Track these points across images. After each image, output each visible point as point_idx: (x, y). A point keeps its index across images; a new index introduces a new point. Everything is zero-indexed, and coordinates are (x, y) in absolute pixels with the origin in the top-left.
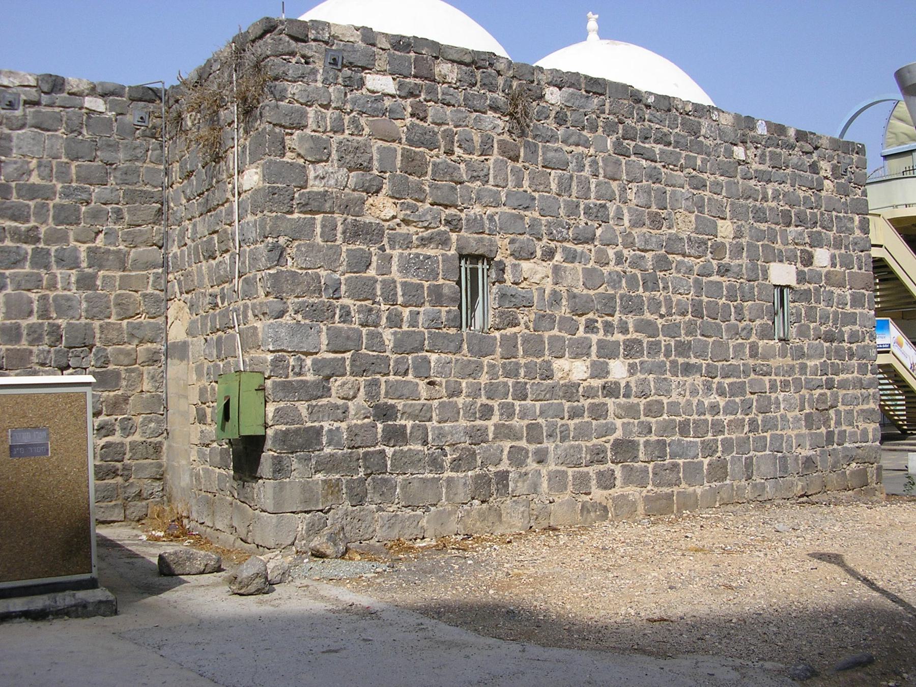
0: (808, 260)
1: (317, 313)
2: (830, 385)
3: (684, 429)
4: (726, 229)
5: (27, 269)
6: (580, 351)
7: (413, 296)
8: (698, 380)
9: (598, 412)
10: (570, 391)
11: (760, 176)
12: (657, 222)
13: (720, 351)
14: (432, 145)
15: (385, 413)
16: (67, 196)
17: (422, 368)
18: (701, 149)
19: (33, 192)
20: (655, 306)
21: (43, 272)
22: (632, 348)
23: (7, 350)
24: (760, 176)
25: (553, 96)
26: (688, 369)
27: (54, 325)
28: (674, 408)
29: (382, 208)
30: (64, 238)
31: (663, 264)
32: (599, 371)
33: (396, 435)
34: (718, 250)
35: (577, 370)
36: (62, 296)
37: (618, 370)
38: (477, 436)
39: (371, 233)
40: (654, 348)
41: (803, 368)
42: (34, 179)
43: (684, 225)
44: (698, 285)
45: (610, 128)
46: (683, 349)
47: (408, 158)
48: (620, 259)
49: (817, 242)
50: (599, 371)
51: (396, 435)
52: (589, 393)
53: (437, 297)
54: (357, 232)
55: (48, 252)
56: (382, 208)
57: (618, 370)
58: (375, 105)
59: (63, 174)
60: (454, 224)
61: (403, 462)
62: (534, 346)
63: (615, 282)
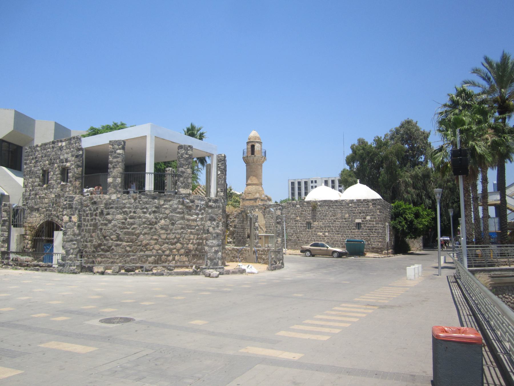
0: (365, 218)
1: (291, 229)
2: (369, 237)
3: (337, 241)
4: (347, 216)
6: (321, 232)
7: (301, 226)
8: (340, 235)
10: (320, 236)
11: (354, 208)
12: (334, 216)
13: (345, 232)
17: (302, 234)
18: (342, 206)
20: (333, 226)
22: (329, 232)
24: (354, 208)
25: (319, 203)
26: (338, 234)
28: (335, 239)
31: (335, 221)
32: (323, 234)
33: (299, 240)
35: (321, 234)
37: (327, 234)
38: (308, 240)
39: (297, 221)
40: (333, 231)
41: (362, 234)
43: (339, 216)
44: (341, 224)
46: (337, 231)
51: (299, 240)
53: (304, 227)
54: (295, 221)
56: (298, 218)
57: (327, 234)
58: (298, 209)
62: (315, 231)
63: (327, 224)
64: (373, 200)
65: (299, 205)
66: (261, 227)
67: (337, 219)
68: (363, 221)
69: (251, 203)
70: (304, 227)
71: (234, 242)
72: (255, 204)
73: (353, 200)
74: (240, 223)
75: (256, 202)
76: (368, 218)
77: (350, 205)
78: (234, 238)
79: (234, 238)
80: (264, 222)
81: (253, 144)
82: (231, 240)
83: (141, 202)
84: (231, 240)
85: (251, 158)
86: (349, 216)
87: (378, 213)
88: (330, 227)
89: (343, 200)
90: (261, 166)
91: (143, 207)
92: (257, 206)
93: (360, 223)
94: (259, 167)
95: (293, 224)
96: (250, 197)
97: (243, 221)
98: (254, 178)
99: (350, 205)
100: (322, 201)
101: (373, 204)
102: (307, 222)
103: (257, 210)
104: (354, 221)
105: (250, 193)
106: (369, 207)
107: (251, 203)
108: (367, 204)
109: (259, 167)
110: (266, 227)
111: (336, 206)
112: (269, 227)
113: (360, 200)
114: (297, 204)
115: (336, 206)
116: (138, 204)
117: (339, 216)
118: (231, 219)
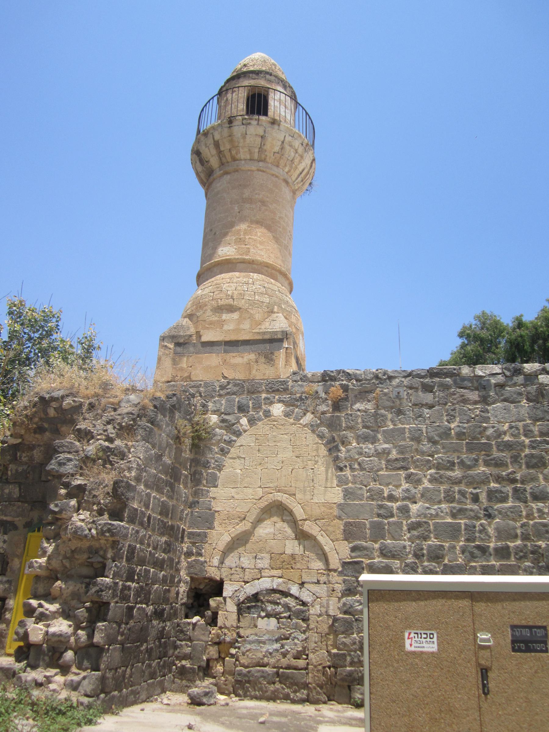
5: (510, 504)
16: (534, 448)
19: (508, 446)
21: (521, 505)
23: (501, 565)
27: (536, 546)
30: (534, 479)
36: (540, 523)
42: (507, 438)
55: (525, 490)
59: (527, 433)
66: (310, 527)
69: (239, 366)
71: (90, 655)
72: (263, 372)
74: (156, 485)
75: (270, 359)
78: (99, 610)
79: (99, 610)
80: (336, 495)
81: (262, 83)
82: (61, 626)
84: (61, 626)
92: (278, 388)
96: (231, 327)
97: (174, 474)
98: (260, 232)
103: (278, 409)
105: (231, 309)
107: (239, 366)
110: (349, 533)
112: (378, 532)
118: (86, 436)
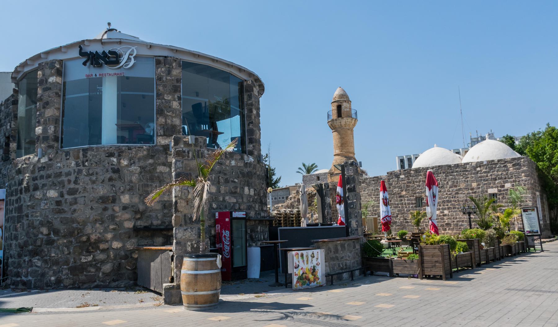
0: (503, 186)
1: (396, 207)
3: (463, 221)
4: (474, 185)
7: (409, 204)
9: (443, 219)
12: (456, 186)
14: (410, 183)
15: (406, 219)
18: (467, 171)
22: (449, 208)
28: (460, 218)
29: (404, 193)
31: (457, 193)
33: (407, 222)
34: (472, 189)
45: (444, 173)
47: (407, 186)
48: (447, 194)
49: (507, 182)
50: (443, 212)
51: (407, 222)
52: (440, 216)
53: (412, 204)
54: (400, 197)
56: (404, 193)
57: (446, 212)
60: (415, 193)
61: (408, 225)
64: (514, 159)
65: (404, 174)
67: (460, 189)
68: (500, 191)
70: (412, 204)
73: (482, 162)
76: (508, 185)
77: (478, 169)
83: (86, 164)
85: (338, 121)
86: (479, 185)
87: (524, 178)
88: (451, 201)
89: (467, 164)
90: (352, 130)
91: (91, 172)
93: (496, 194)
94: (349, 132)
95: (397, 201)
99: (478, 169)
100: (436, 167)
101: (514, 165)
102: (416, 198)
104: (487, 191)
106: (508, 170)
108: (505, 166)
109: (349, 132)
111: (457, 172)
113: (493, 161)
114: (400, 174)
115: (457, 172)
116: (81, 167)
117: (462, 186)
